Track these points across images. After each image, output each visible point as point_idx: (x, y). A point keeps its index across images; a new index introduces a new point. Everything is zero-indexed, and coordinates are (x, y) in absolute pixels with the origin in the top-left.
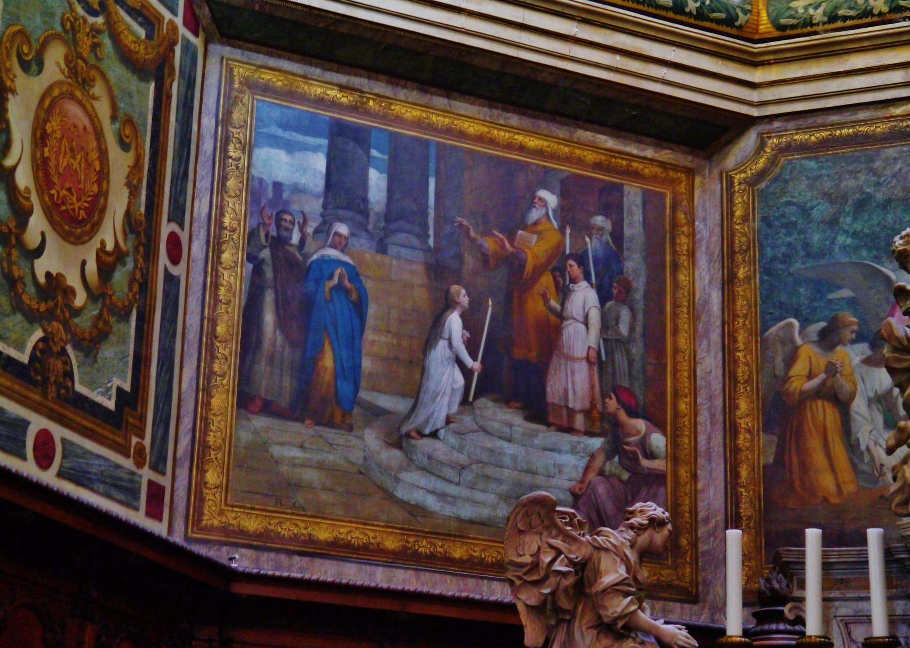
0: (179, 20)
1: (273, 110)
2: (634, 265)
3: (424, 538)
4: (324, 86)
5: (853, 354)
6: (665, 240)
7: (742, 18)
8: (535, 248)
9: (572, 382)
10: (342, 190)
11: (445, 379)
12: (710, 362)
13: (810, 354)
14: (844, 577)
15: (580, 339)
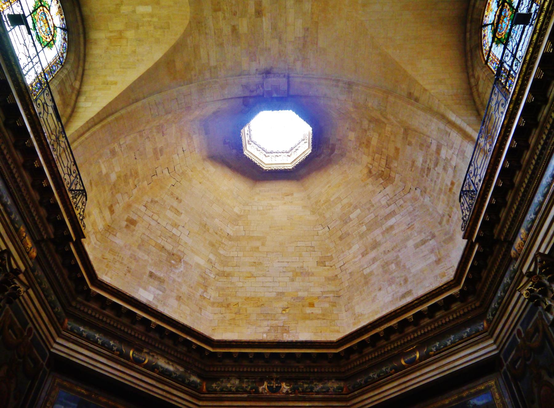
0: (44, 364)
7: (199, 387)
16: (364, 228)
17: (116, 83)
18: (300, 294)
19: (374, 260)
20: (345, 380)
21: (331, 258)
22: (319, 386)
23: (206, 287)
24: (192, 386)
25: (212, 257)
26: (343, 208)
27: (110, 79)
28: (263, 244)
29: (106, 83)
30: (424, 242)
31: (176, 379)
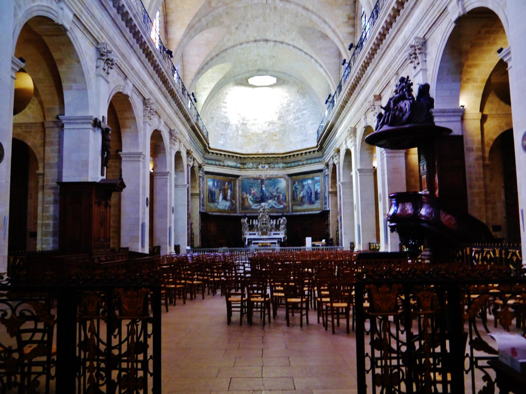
1: (209, 179)
3: (220, 211)
4: (212, 176)
5: (248, 195)
6: (235, 186)
8: (226, 187)
9: (229, 198)
11: (221, 197)
14: (255, 221)
15: (229, 194)
16: (295, 111)
17: (207, 88)
18: (272, 131)
19: (297, 124)
20: (285, 163)
21: (283, 117)
22: (277, 166)
23: (238, 131)
24: (239, 168)
26: (288, 100)
27: (205, 86)
29: (203, 88)
30: (313, 124)
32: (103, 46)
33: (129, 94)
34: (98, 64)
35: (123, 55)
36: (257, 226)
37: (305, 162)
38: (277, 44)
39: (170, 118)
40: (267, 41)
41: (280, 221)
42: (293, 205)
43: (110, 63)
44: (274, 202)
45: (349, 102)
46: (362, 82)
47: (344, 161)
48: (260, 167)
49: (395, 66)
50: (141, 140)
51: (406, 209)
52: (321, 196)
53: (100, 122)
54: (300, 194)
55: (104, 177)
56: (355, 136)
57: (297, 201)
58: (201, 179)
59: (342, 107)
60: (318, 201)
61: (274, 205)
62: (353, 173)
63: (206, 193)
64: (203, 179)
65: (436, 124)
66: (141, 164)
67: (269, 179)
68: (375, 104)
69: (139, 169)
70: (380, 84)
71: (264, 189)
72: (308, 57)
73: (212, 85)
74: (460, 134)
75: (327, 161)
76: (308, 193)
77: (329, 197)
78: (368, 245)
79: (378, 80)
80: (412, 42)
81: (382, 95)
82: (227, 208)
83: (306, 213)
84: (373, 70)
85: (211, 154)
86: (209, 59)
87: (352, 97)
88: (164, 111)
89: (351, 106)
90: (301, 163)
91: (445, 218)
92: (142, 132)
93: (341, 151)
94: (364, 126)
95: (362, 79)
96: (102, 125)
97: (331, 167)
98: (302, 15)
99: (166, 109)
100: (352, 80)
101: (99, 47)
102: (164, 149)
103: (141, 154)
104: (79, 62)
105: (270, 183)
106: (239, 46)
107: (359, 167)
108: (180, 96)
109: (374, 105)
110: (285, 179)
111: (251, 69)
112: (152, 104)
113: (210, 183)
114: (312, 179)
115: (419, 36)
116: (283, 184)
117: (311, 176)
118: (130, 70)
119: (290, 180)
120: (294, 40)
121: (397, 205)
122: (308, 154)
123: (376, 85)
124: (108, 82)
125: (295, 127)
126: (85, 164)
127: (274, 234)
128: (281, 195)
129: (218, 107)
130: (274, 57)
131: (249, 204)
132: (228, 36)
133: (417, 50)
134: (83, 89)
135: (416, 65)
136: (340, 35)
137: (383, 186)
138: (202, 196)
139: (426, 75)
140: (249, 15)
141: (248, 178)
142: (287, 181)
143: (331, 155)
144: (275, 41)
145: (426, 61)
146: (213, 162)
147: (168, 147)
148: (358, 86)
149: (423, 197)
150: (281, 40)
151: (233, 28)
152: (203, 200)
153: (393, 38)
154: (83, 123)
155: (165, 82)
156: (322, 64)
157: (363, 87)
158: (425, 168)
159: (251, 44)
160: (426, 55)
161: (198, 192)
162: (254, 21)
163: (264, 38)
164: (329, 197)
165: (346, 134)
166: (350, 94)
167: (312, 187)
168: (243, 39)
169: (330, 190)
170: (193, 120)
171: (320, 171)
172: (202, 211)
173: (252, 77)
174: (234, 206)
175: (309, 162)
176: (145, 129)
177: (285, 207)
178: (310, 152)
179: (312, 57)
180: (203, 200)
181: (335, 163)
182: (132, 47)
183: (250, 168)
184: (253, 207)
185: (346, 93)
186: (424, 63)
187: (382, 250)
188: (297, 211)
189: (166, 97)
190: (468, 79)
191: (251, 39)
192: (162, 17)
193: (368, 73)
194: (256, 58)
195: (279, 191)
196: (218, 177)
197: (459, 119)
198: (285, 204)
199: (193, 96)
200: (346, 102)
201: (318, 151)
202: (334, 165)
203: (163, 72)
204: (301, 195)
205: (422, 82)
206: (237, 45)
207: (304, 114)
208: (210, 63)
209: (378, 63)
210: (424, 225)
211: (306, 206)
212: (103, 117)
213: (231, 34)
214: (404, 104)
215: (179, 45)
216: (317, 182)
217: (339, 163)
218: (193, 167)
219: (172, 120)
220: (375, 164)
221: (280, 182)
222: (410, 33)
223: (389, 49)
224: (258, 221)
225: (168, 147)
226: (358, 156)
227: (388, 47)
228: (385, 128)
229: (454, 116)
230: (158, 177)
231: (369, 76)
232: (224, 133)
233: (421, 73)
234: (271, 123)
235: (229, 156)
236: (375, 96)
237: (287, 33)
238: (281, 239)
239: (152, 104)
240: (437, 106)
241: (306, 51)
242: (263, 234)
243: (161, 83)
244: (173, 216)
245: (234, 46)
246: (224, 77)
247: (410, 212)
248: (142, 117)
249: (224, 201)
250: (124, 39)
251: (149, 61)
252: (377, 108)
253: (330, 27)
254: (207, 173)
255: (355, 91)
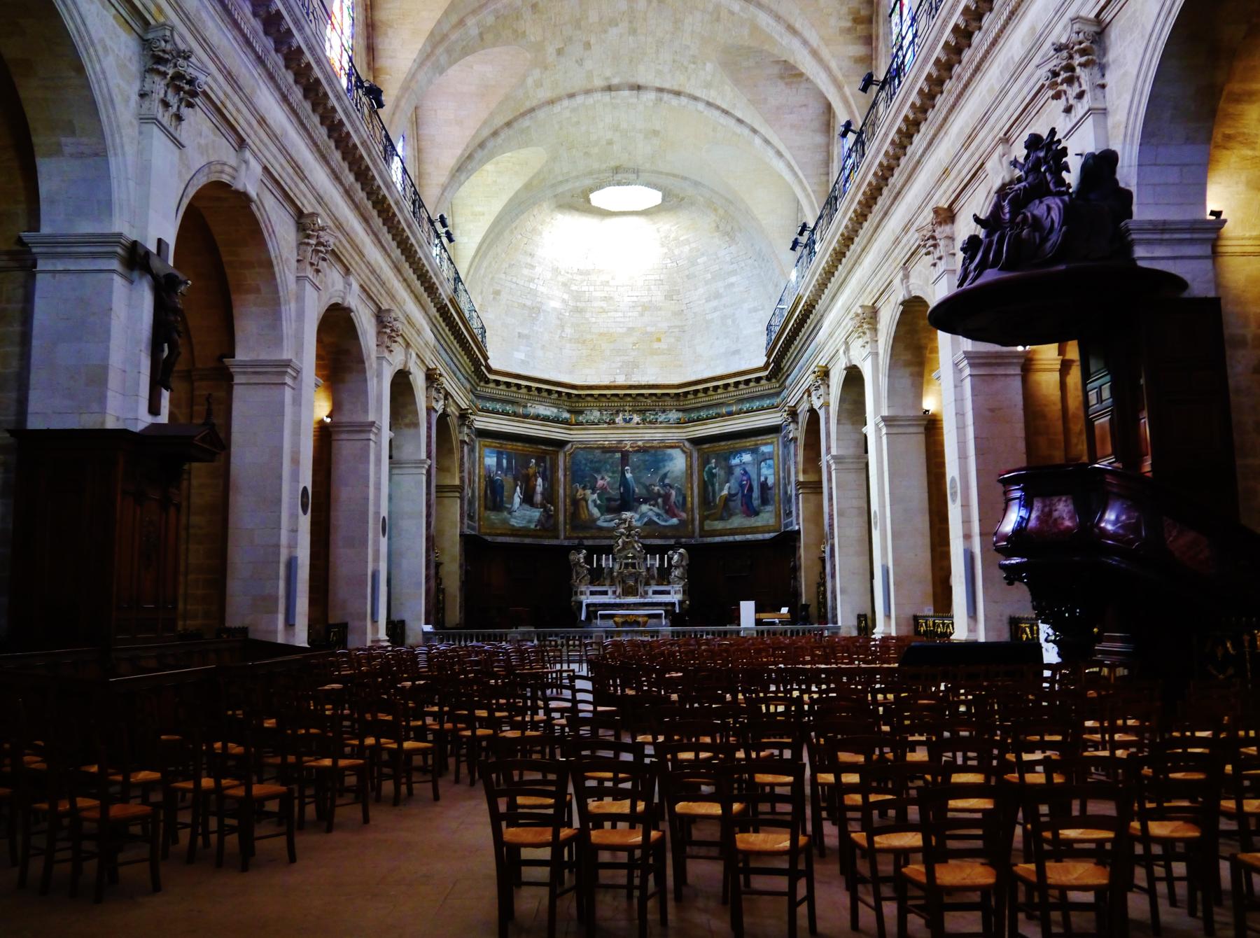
1: (487, 451)
2: (548, 473)
3: (515, 532)
4: (496, 443)
5: (588, 492)
8: (531, 471)
9: (538, 498)
10: (499, 463)
11: (517, 500)
12: (561, 491)
13: (580, 492)
14: (607, 559)
15: (539, 489)
16: (709, 276)
18: (649, 329)
19: (715, 309)
20: (684, 411)
21: (678, 293)
22: (662, 417)
23: (562, 327)
24: (565, 422)
25: (566, 296)
26: (691, 250)
27: (478, 209)
28: (613, 279)
30: (755, 310)
31: (552, 421)
32: (160, 33)
33: (253, 193)
34: (147, 88)
35: (230, 77)
36: (611, 570)
37: (734, 408)
38: (666, 96)
39: (378, 278)
40: (639, 88)
41: (670, 559)
42: (703, 519)
43: (187, 87)
44: (655, 509)
45: (856, 240)
46: (896, 179)
47: (842, 400)
48: (619, 419)
49: (1001, 117)
50: (288, 328)
51: (1056, 514)
52: (777, 494)
53: (148, 253)
54: (721, 490)
55: (164, 418)
56: (876, 330)
57: (716, 506)
58: (466, 448)
59: (839, 255)
60: (769, 508)
61: (655, 519)
62: (870, 430)
63: (479, 485)
64: (472, 450)
65: (1141, 264)
66: (288, 393)
67: (643, 450)
68: (936, 234)
69: (283, 406)
70: (963, 164)
71: (629, 475)
72: (746, 132)
73: (497, 206)
74: (1212, 294)
75: (792, 404)
76: (742, 486)
77: (797, 496)
78: (912, 622)
79: (945, 165)
80: (1061, 33)
81: (956, 207)
82: (532, 526)
83: (738, 538)
84: (930, 143)
85: (492, 385)
86: (486, 132)
87: (866, 225)
88: (361, 254)
89: (863, 250)
90: (724, 410)
91: (1179, 540)
92: (293, 305)
93: (832, 374)
94: (901, 299)
95: (896, 172)
96: (155, 264)
97: (803, 418)
98: (732, 13)
99: (366, 252)
100: (870, 177)
101: (150, 36)
102: (361, 361)
103: (287, 364)
104: (80, 69)
105: (645, 461)
106: (566, 103)
107: (885, 412)
108: (406, 220)
109: (933, 238)
110: (684, 452)
111: (596, 166)
112: (323, 229)
113: (491, 461)
114: (754, 451)
115: (1083, 14)
116: (678, 463)
117: (749, 442)
118: (254, 123)
119: (695, 455)
120: (708, 85)
121: (1027, 504)
122: (742, 386)
123: (940, 181)
124: (180, 145)
125: (709, 317)
126: (98, 378)
127: (655, 592)
128: (673, 493)
129: (511, 266)
130: (656, 133)
131: (591, 515)
132: (536, 73)
133: (1077, 56)
134: (97, 155)
135: (1071, 101)
136: (833, 65)
137: (963, 457)
138: (468, 492)
139: (1105, 127)
140: (593, 17)
141: (588, 448)
142: (689, 456)
143: (805, 387)
144: (660, 90)
145: (1103, 86)
146: (498, 406)
147: (374, 355)
148: (885, 191)
149: (1109, 479)
150: (676, 88)
151: (551, 50)
152: (471, 503)
153: (994, 43)
154: (94, 256)
155: (363, 175)
156: (782, 148)
157: (899, 193)
158: (1106, 394)
159: (598, 96)
160: (1103, 68)
161: (457, 482)
162: (606, 32)
163: (632, 80)
164: (797, 496)
165: (849, 324)
166: (861, 216)
167: (752, 471)
168: (577, 81)
169: (801, 479)
170: (445, 291)
171: (775, 429)
172: (468, 531)
173: (599, 187)
174: (552, 522)
175: (746, 406)
176: (300, 299)
177: (683, 523)
178: (747, 382)
179: (754, 131)
180: (471, 503)
181: (816, 407)
182: (260, 60)
183: (593, 423)
184: (600, 523)
185: (850, 214)
186: (1099, 91)
187: (960, 633)
188: (714, 533)
189: (366, 220)
190: (1228, 138)
191: (599, 82)
192: (360, 10)
193: (914, 154)
194: (609, 135)
195: (667, 481)
196: (510, 445)
197: (1207, 250)
198: (684, 515)
199: (444, 225)
200: (848, 240)
201: (768, 378)
202: (813, 413)
203: (355, 146)
204: (725, 492)
205: (1091, 147)
206: (559, 99)
207: (732, 284)
208: (490, 145)
209: (945, 119)
210: (1113, 561)
211: (737, 521)
212: (160, 241)
213: (546, 68)
214: (1043, 207)
215: (405, 88)
216: (765, 460)
217: (826, 405)
218: (444, 416)
219: (383, 284)
220: (930, 403)
221: (671, 458)
222: (1052, 13)
223: (979, 76)
224: (614, 559)
225: (374, 355)
226: (884, 382)
227: (977, 69)
228: (990, 275)
229: (1192, 241)
230: (344, 436)
231: (918, 162)
232: (526, 332)
233: (1090, 121)
234: (646, 308)
235: (539, 390)
236: (937, 211)
237: (693, 66)
238: (673, 604)
239: (323, 229)
240: (1141, 212)
241: (739, 115)
242: (626, 592)
243: (351, 178)
244: (384, 541)
245: (552, 102)
246: (528, 187)
247: (1068, 523)
248: (294, 263)
249: (526, 506)
250: (236, 32)
251: (314, 110)
252: (942, 243)
253: (805, 42)
254: (483, 433)
255: (876, 208)
